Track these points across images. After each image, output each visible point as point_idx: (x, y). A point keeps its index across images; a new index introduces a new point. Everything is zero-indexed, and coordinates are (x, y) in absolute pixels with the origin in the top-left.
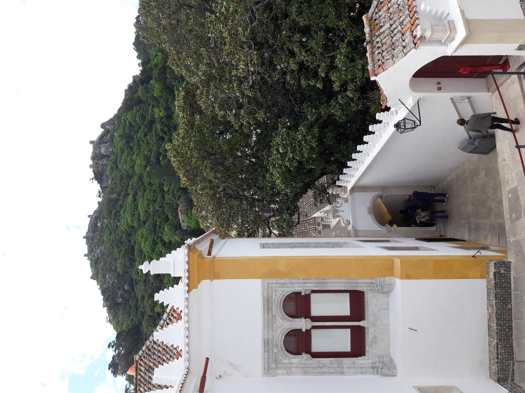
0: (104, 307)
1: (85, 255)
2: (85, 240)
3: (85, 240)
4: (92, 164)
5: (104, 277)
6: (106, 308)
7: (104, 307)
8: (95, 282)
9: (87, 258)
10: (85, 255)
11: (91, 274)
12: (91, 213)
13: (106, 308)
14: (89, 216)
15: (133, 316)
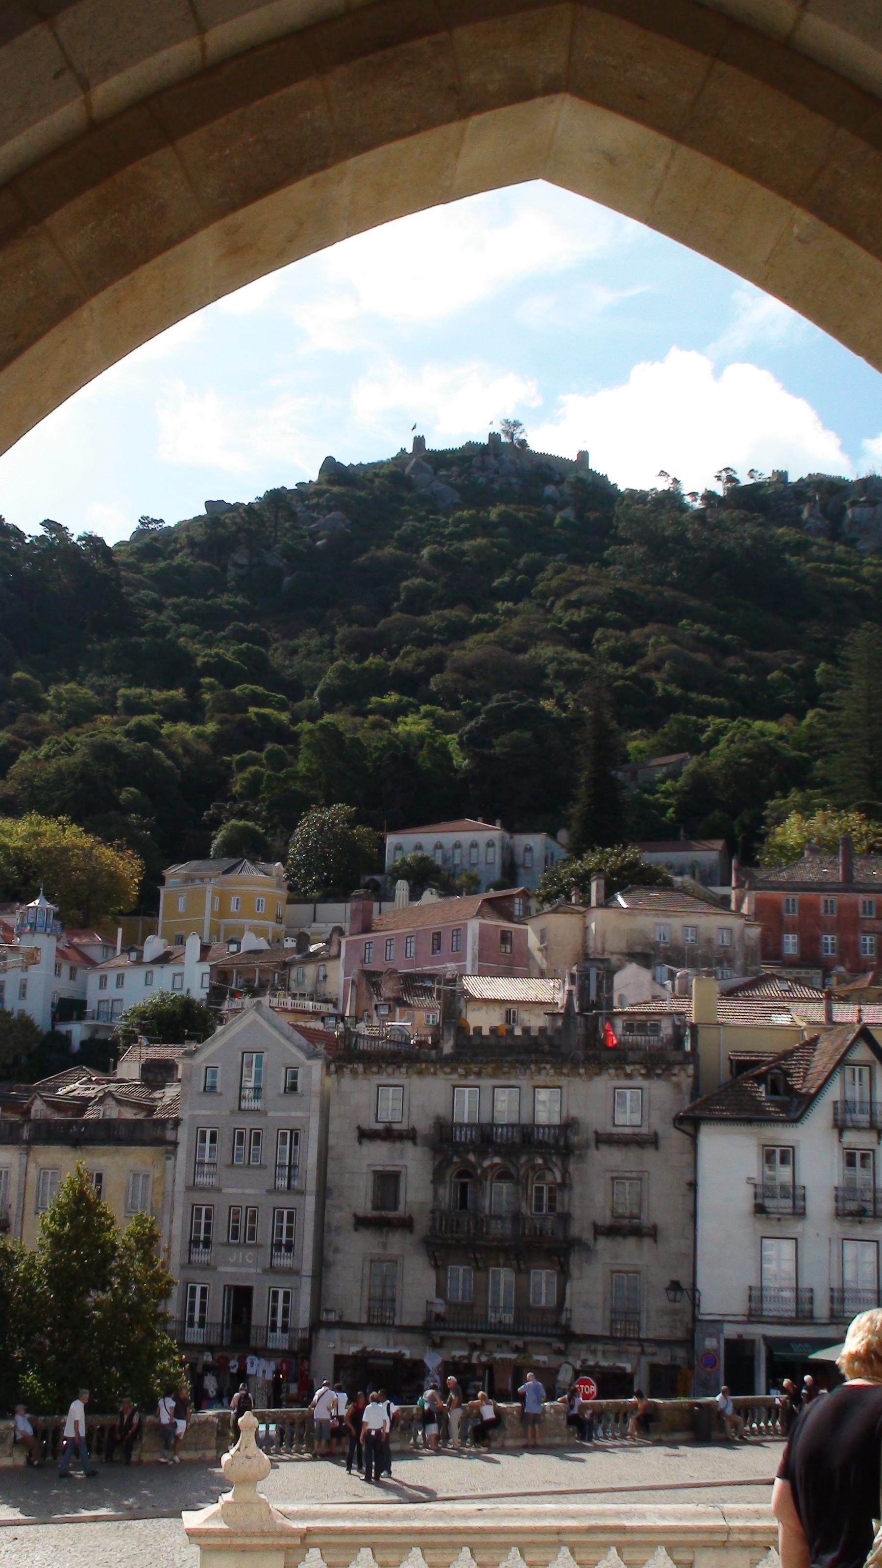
0: (209, 504)
1: (419, 442)
2: (485, 441)
3: (485, 441)
4: (793, 478)
5: (337, 504)
6: (203, 512)
7: (209, 504)
8: (311, 474)
9: (410, 450)
10: (419, 442)
11: (346, 459)
12: (596, 465)
13: (203, 512)
14: (583, 456)
15: (176, 607)
